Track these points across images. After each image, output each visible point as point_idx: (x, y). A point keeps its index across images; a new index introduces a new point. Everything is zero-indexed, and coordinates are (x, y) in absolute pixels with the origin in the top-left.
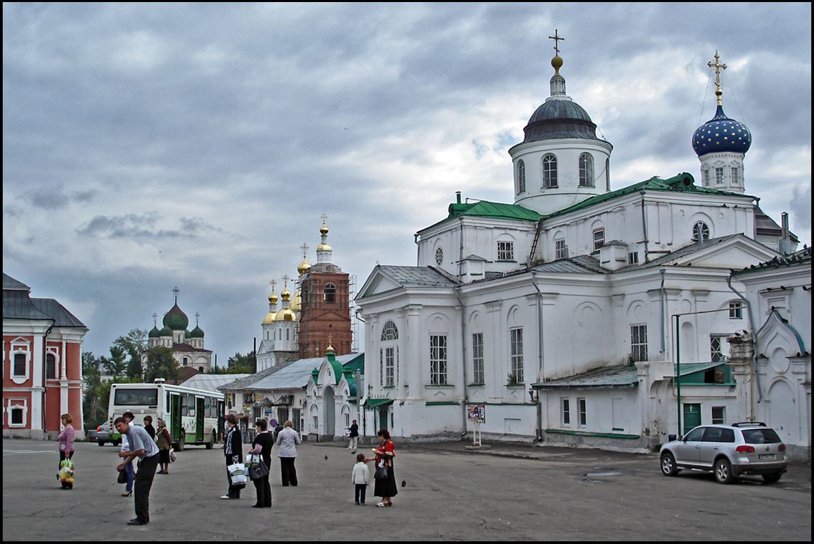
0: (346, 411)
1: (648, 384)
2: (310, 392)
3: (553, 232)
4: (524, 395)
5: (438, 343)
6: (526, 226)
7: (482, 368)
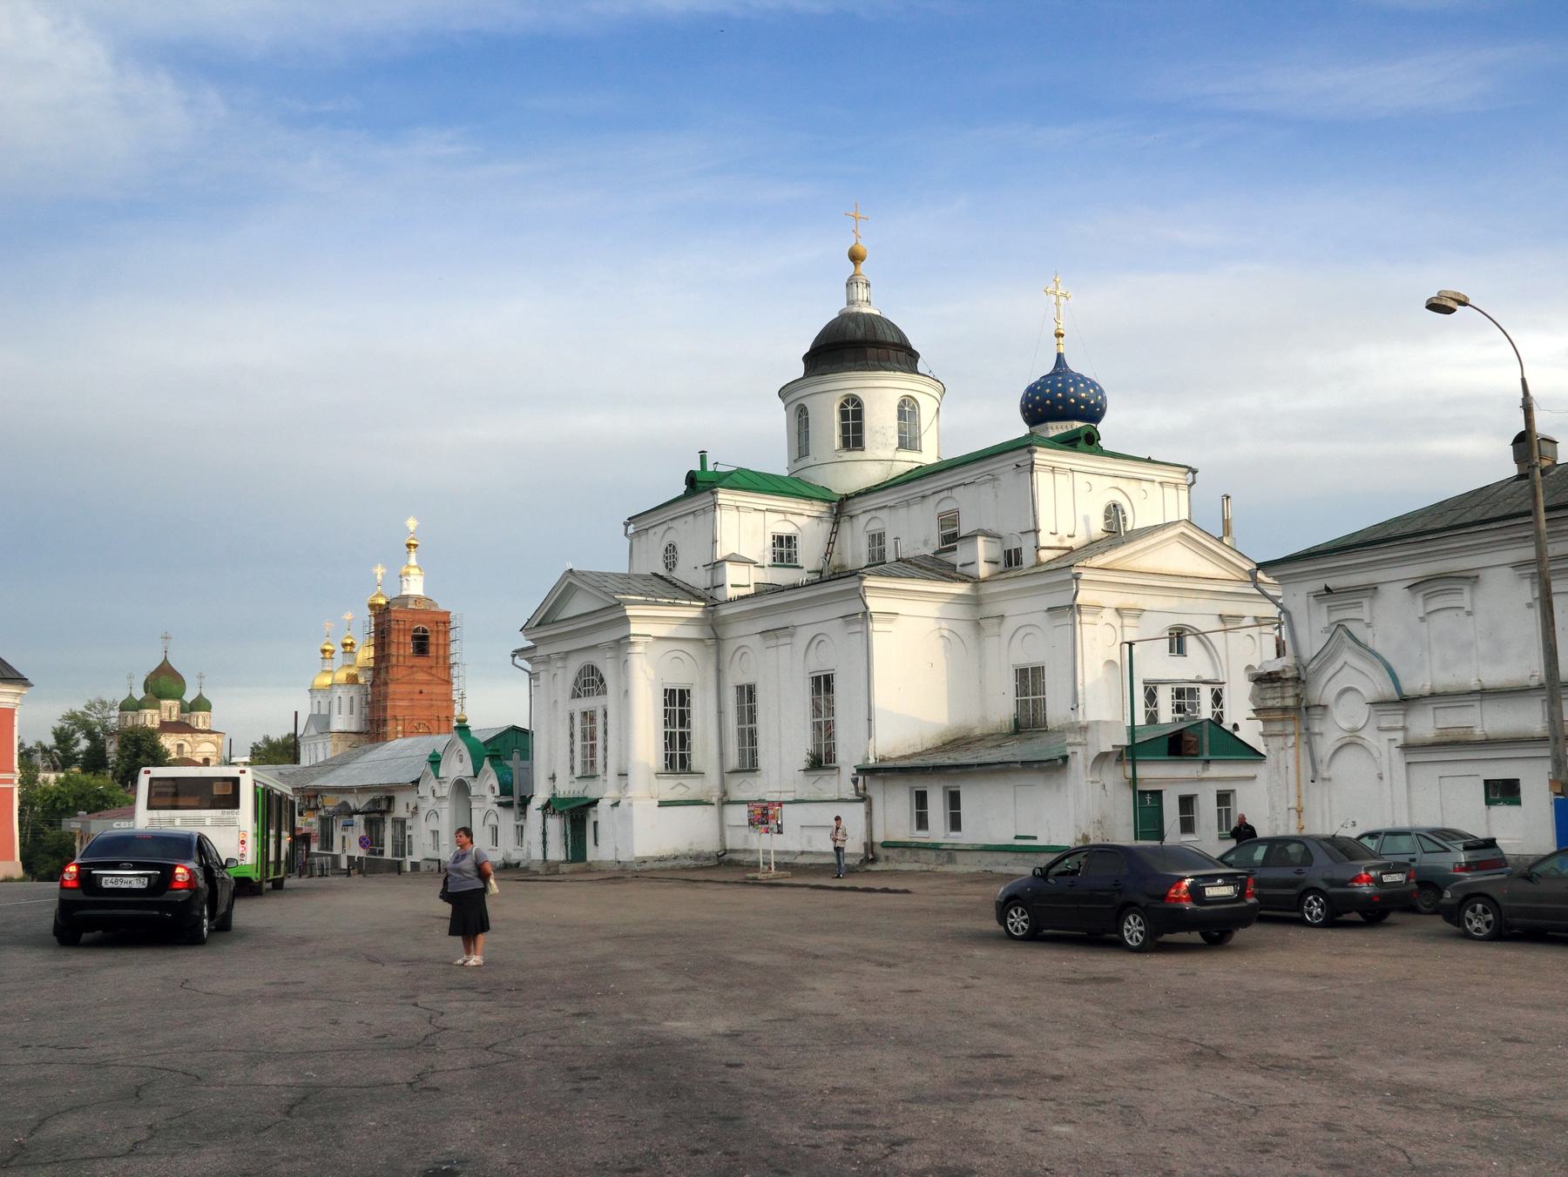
0: (492, 820)
1: (1086, 759)
2: (424, 790)
3: (863, 519)
4: (842, 783)
5: (677, 702)
6: (817, 508)
7: (753, 742)
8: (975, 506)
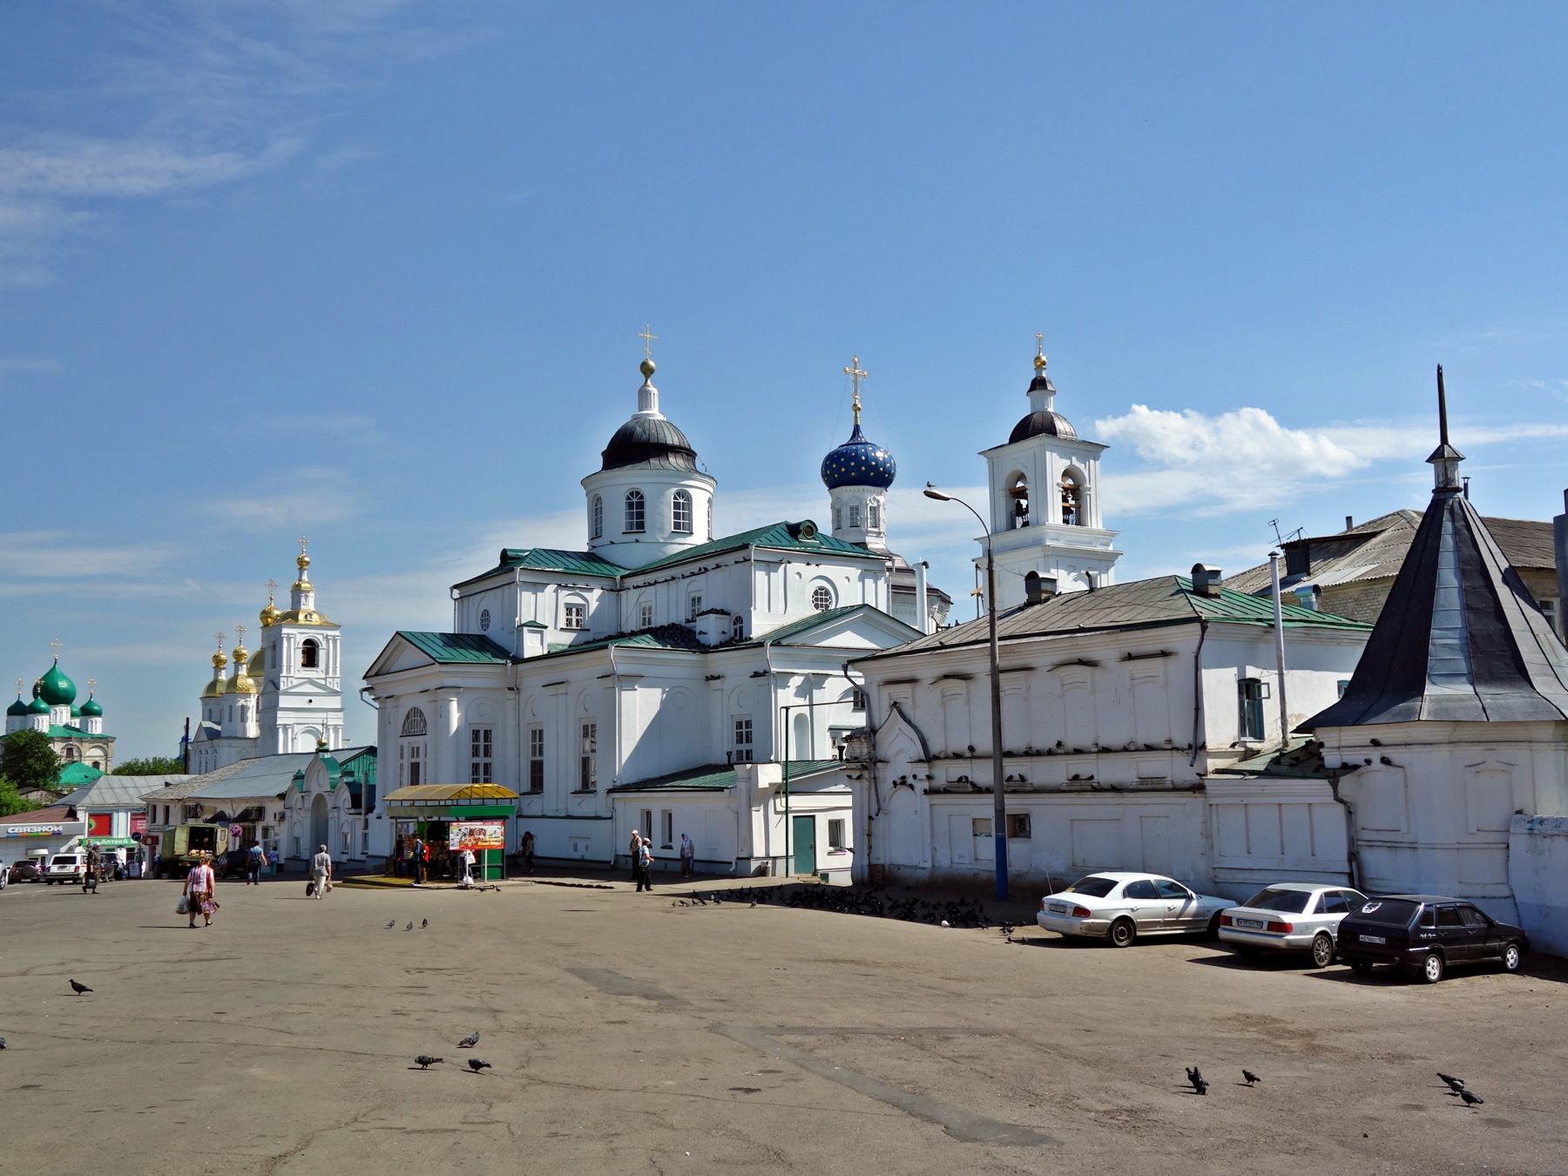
8: (713, 587)
